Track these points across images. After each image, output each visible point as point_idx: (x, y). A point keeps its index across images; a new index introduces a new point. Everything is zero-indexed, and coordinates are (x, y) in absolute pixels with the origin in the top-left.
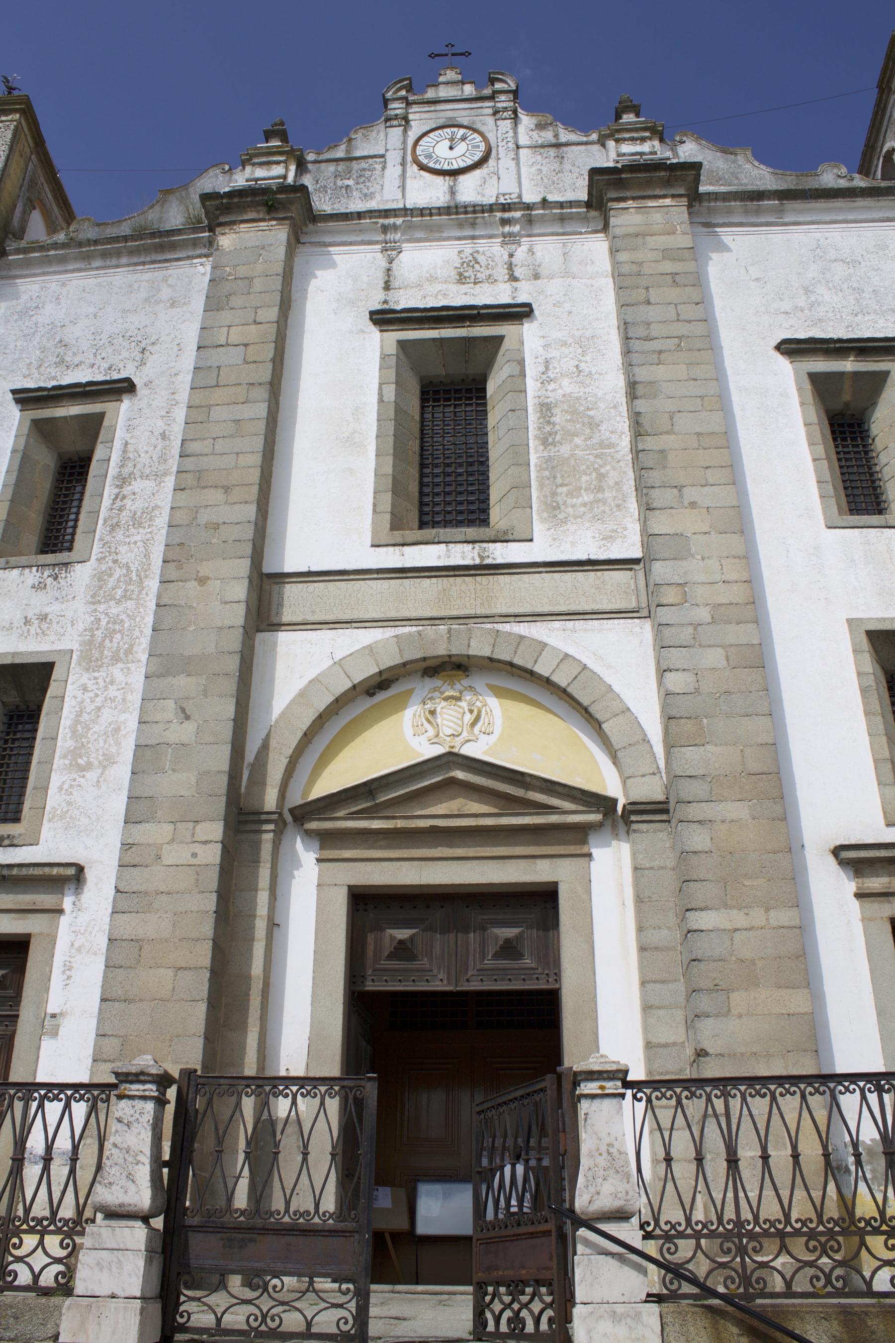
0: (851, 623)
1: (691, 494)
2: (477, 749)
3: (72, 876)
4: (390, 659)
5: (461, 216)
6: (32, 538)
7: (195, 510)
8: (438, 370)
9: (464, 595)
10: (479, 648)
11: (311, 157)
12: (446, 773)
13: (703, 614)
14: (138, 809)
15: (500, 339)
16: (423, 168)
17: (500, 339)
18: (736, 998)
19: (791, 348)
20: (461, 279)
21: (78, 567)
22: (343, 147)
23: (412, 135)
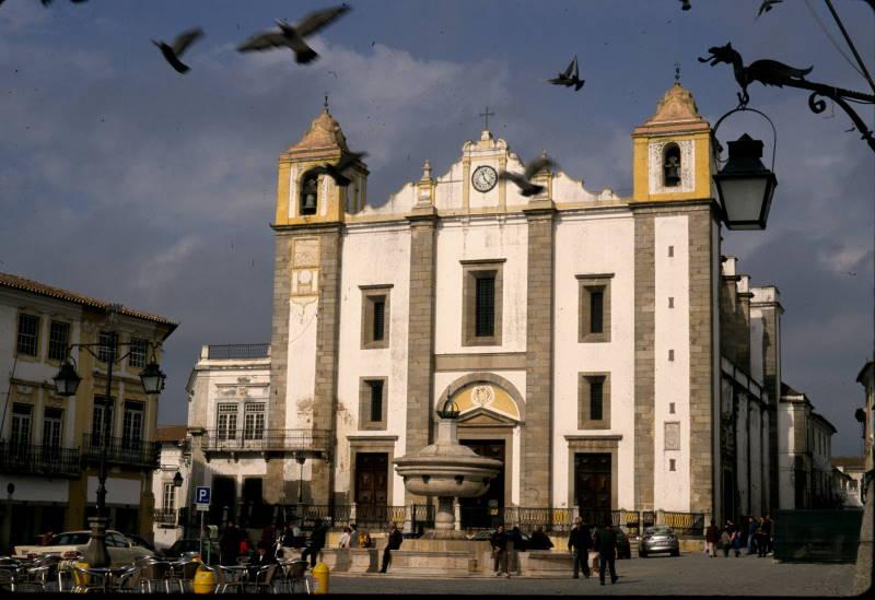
0: (580, 373)
1: (539, 339)
2: (487, 406)
3: (396, 438)
4: (466, 382)
5: (487, 216)
6: (371, 335)
7: (414, 340)
8: (480, 276)
9: (485, 362)
10: (488, 379)
11: (439, 180)
12: (480, 412)
13: (536, 376)
14: (409, 425)
15: (495, 271)
16: (475, 188)
17: (495, 271)
18: (534, 472)
19: (579, 277)
20: (487, 245)
21: (385, 350)
22: (448, 175)
23: (472, 171)
